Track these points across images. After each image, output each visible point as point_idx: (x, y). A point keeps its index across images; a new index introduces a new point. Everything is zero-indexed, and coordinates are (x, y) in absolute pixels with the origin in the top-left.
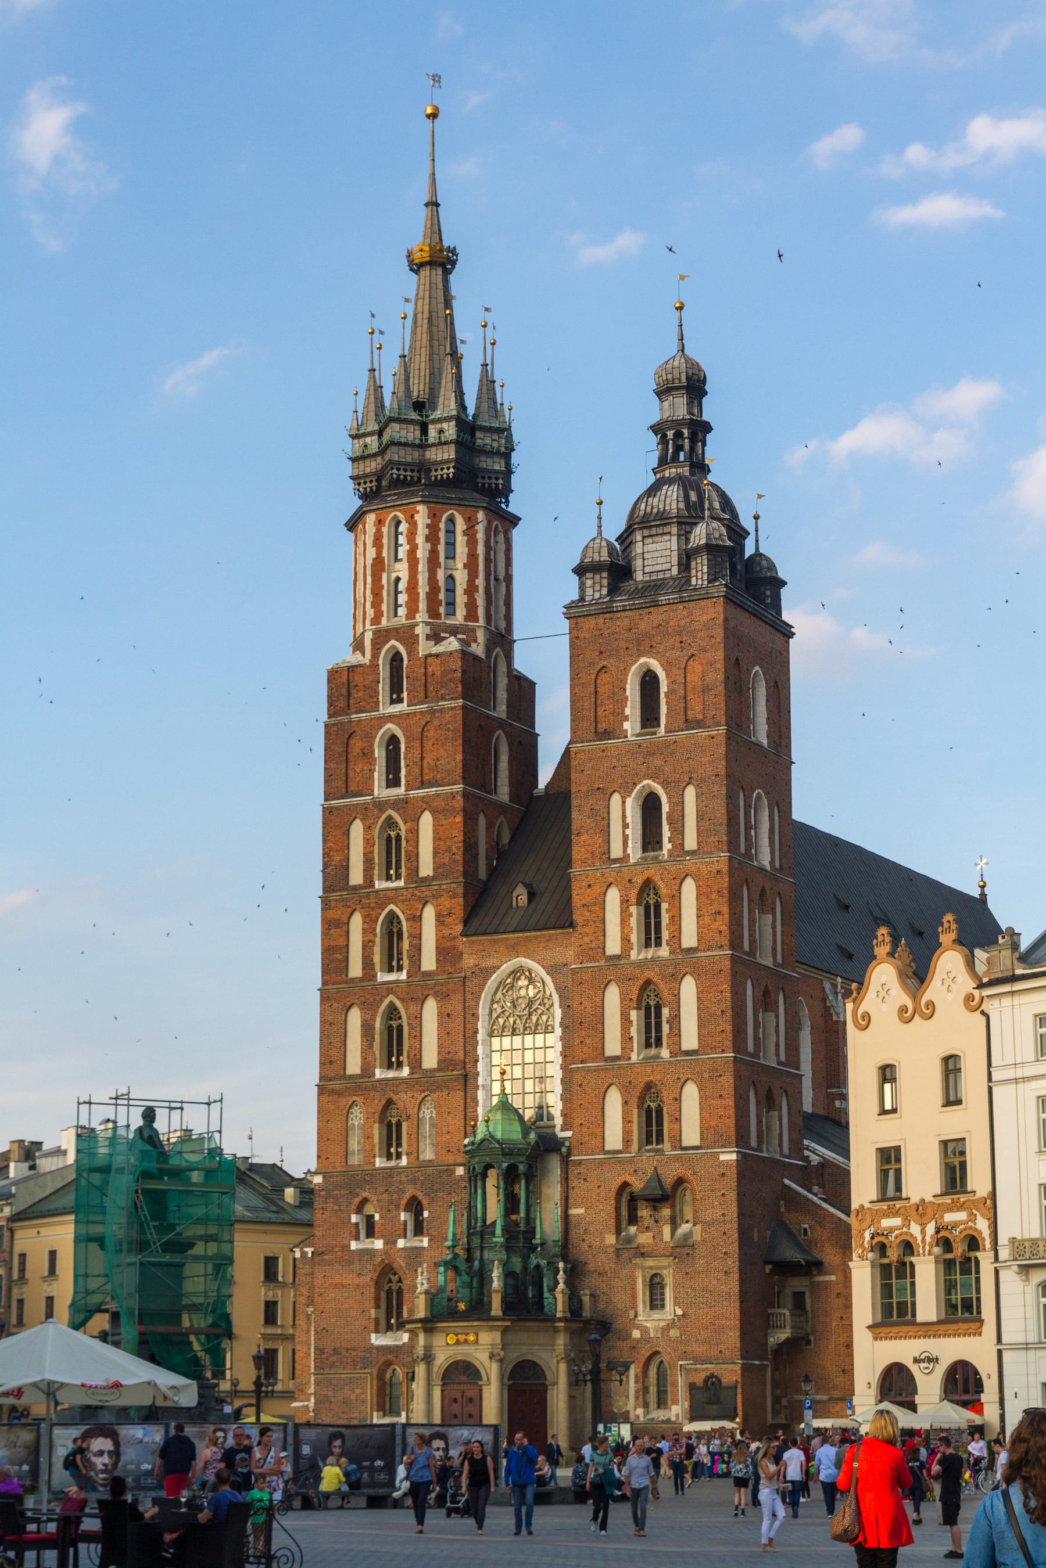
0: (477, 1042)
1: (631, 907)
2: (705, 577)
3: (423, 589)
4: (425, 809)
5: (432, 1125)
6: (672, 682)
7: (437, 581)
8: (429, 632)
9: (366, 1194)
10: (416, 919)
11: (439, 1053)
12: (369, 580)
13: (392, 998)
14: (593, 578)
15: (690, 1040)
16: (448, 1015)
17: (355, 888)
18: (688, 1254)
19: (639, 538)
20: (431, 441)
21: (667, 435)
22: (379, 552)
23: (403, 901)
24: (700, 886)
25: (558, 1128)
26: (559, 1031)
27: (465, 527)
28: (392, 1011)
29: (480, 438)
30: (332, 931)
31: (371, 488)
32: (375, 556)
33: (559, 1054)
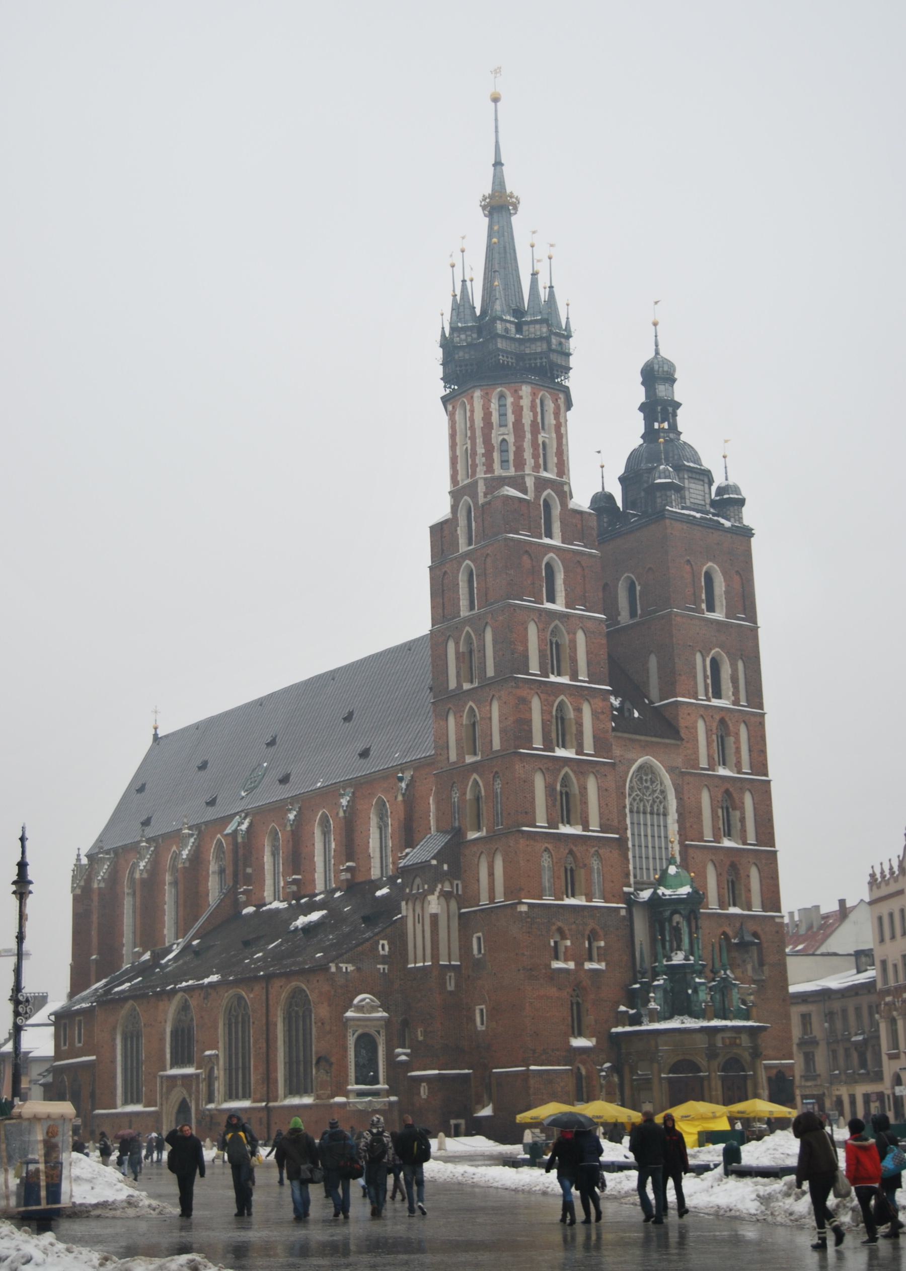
0: (626, 814)
4: (581, 628)
5: (598, 873)
6: (727, 586)
9: (559, 924)
10: (579, 710)
11: (601, 818)
12: (528, 436)
13: (566, 769)
16: (606, 790)
18: (762, 986)
19: (686, 476)
21: (668, 410)
28: (565, 781)
30: (521, 706)
31: (512, 363)
33: (676, 833)
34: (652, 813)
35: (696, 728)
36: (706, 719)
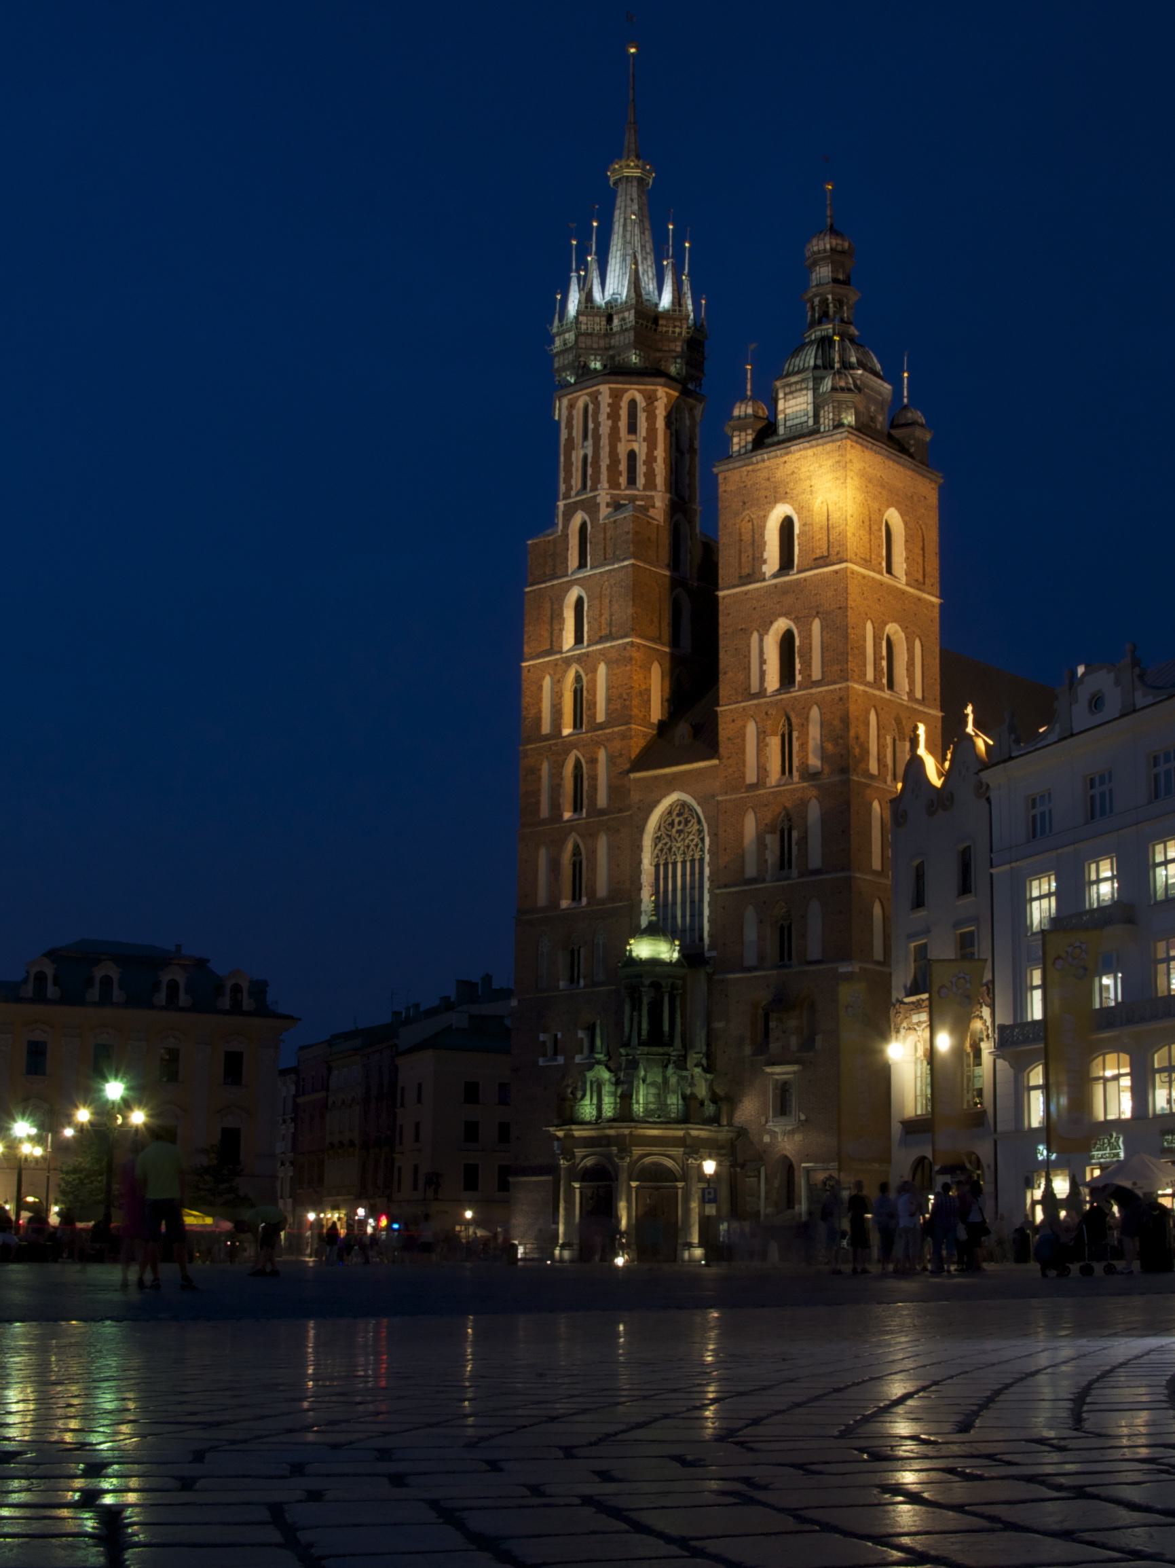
1: (767, 738)
2: (831, 423)
3: (605, 462)
7: (617, 455)
8: (609, 500)
10: (593, 761)
14: (739, 436)
15: (815, 861)
17: (547, 738)
20: (615, 329)
22: (570, 433)
23: (584, 746)
24: (825, 713)
25: (706, 947)
26: (707, 858)
27: (644, 404)
29: (662, 325)
32: (566, 437)
34: (684, 862)
35: (743, 738)
36: (757, 719)
